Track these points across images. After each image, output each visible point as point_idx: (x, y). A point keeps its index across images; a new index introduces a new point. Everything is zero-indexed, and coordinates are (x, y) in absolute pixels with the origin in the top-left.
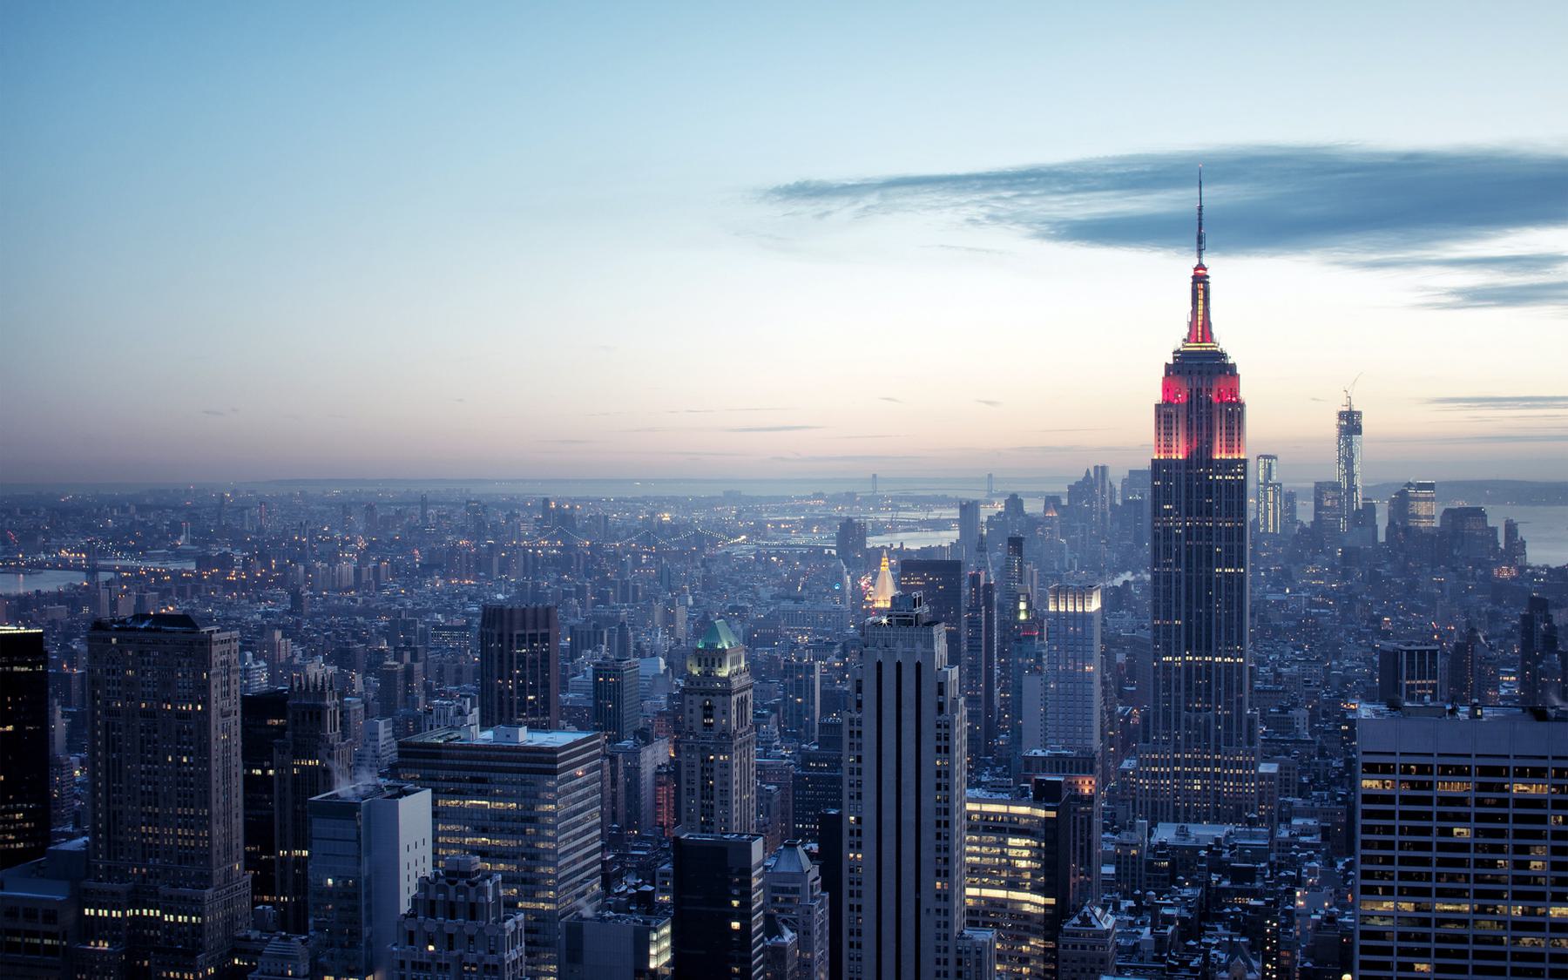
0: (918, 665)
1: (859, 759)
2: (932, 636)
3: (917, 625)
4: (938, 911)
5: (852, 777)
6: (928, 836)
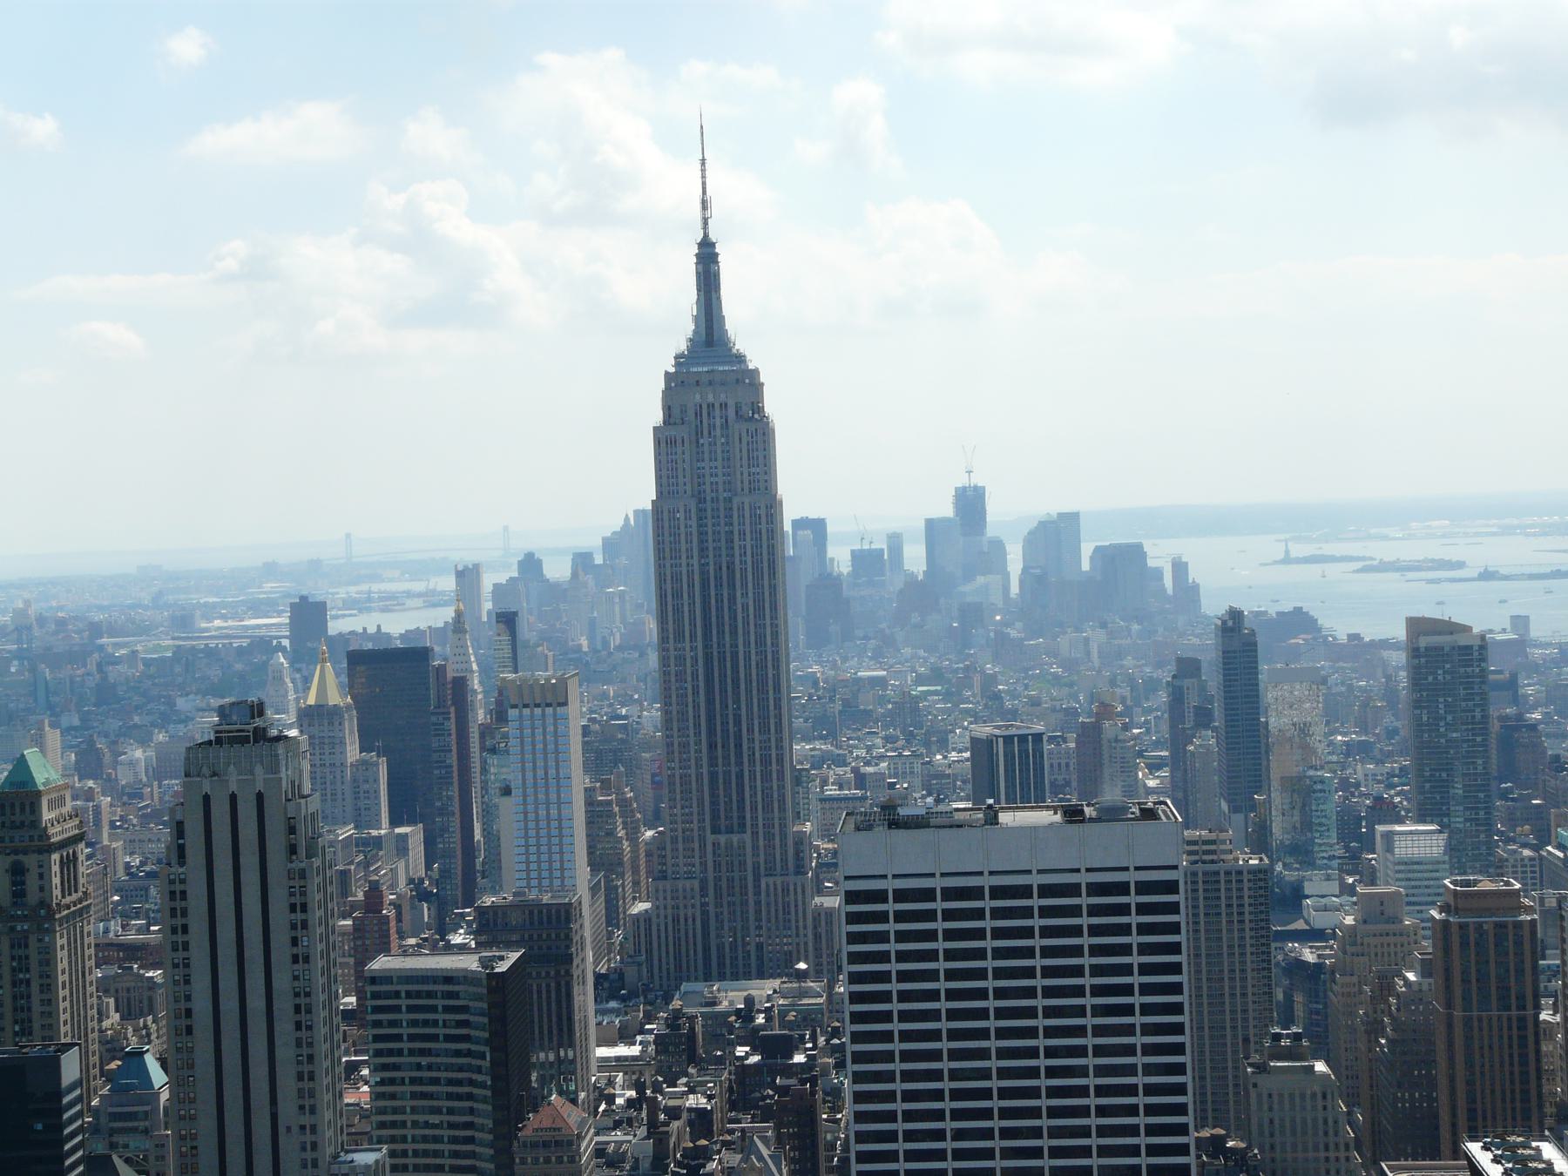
0: (260, 797)
1: (185, 929)
2: (277, 755)
3: (256, 741)
4: (303, 1128)
5: (175, 955)
6: (284, 1027)
